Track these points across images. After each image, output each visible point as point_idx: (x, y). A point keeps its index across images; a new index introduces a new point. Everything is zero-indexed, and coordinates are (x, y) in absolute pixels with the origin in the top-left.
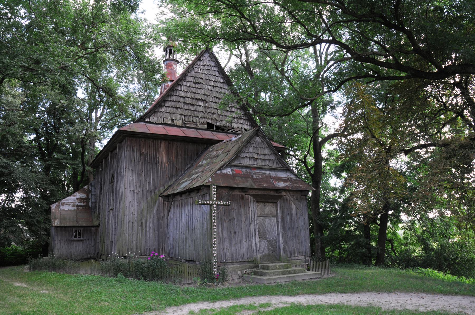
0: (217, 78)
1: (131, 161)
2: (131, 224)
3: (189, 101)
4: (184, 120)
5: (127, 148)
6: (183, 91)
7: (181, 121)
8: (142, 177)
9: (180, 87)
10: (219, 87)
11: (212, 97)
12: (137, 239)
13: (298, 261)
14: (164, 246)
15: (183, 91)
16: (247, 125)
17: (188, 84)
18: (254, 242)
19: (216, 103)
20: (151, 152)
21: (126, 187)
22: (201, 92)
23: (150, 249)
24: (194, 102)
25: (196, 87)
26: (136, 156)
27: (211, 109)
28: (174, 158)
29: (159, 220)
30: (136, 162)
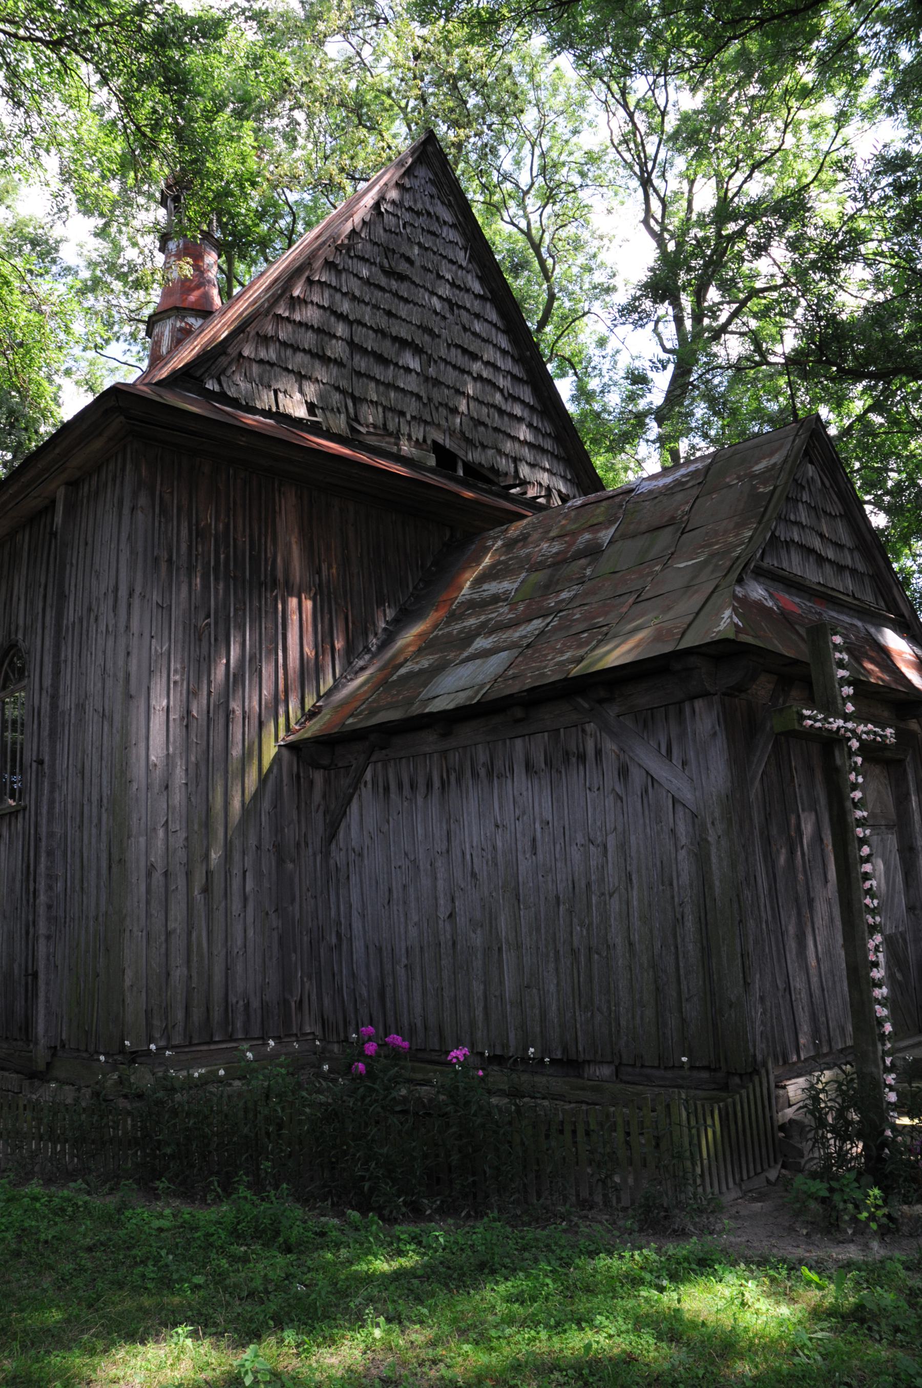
0: (460, 272)
1: (156, 560)
2: (162, 879)
3: (370, 342)
4: (352, 415)
5: (135, 495)
6: (345, 294)
7: (343, 416)
8: (205, 644)
9: (333, 273)
10: (468, 310)
11: (449, 345)
12: (189, 961)
14: (307, 985)
15: (345, 294)
20: (240, 528)
21: (133, 692)
22: (410, 313)
23: (247, 1006)
24: (388, 349)
25: (390, 291)
26: (178, 541)
27: (446, 391)
28: (334, 571)
29: (280, 862)
30: (178, 569)
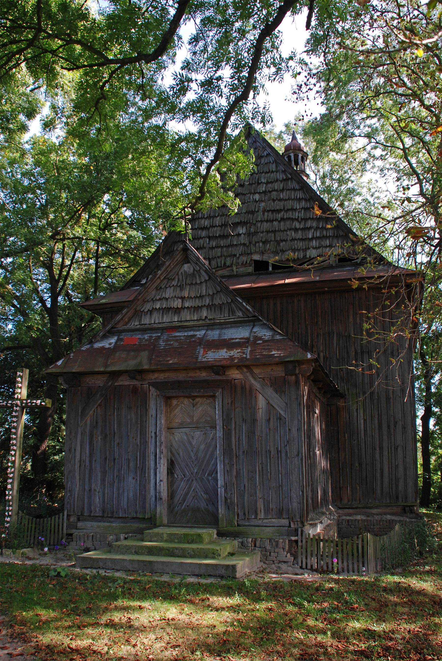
10: (277, 191)
13: (268, 529)
19: (272, 221)
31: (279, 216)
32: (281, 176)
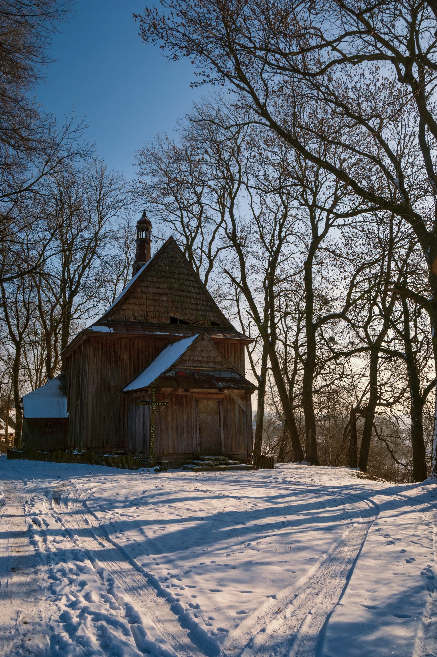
16: (214, 317)
17: (151, 279)
18: (195, 437)
19: (180, 296)
31: (184, 294)
32: (186, 272)
